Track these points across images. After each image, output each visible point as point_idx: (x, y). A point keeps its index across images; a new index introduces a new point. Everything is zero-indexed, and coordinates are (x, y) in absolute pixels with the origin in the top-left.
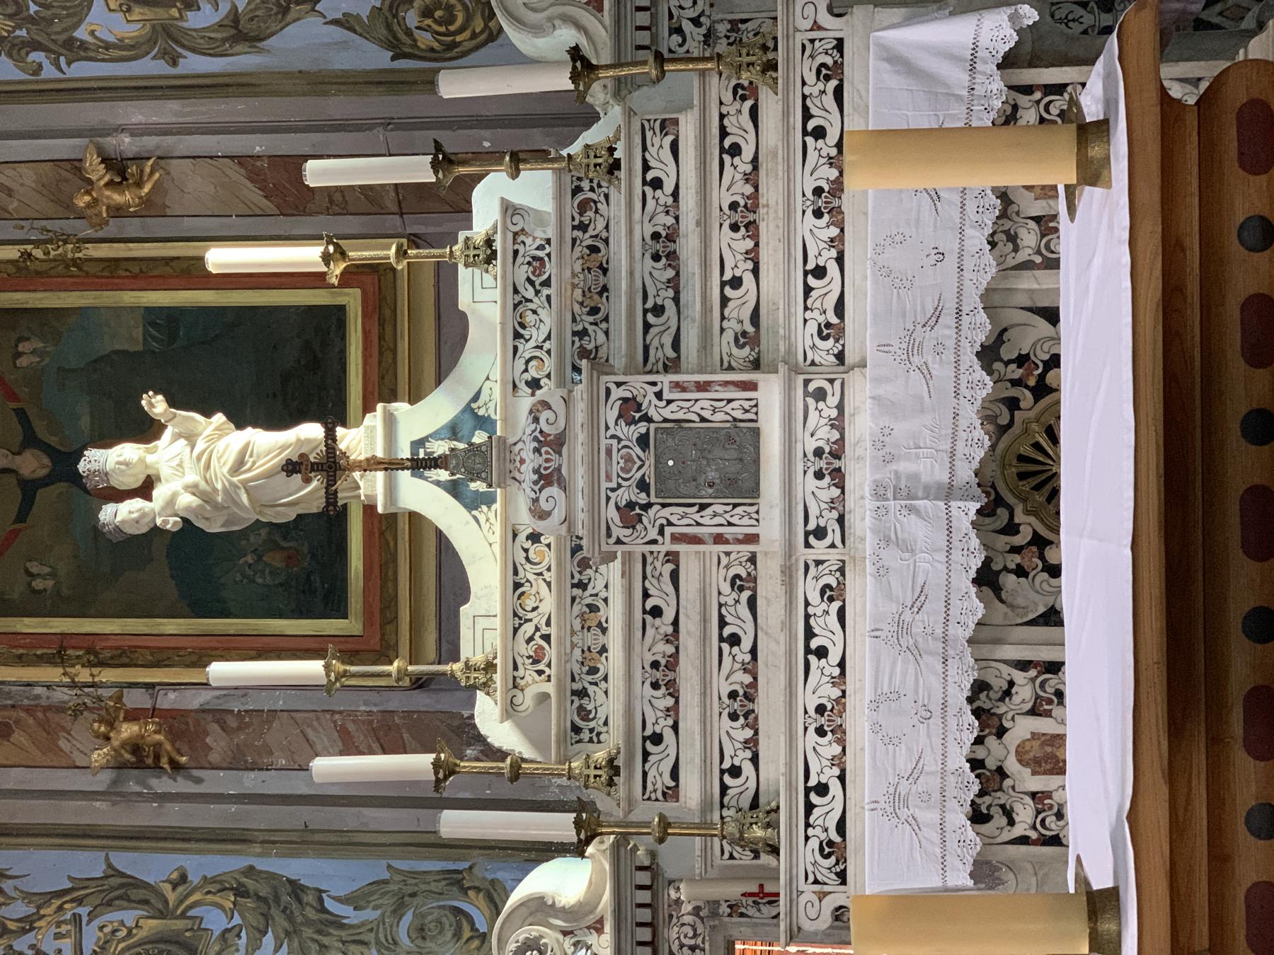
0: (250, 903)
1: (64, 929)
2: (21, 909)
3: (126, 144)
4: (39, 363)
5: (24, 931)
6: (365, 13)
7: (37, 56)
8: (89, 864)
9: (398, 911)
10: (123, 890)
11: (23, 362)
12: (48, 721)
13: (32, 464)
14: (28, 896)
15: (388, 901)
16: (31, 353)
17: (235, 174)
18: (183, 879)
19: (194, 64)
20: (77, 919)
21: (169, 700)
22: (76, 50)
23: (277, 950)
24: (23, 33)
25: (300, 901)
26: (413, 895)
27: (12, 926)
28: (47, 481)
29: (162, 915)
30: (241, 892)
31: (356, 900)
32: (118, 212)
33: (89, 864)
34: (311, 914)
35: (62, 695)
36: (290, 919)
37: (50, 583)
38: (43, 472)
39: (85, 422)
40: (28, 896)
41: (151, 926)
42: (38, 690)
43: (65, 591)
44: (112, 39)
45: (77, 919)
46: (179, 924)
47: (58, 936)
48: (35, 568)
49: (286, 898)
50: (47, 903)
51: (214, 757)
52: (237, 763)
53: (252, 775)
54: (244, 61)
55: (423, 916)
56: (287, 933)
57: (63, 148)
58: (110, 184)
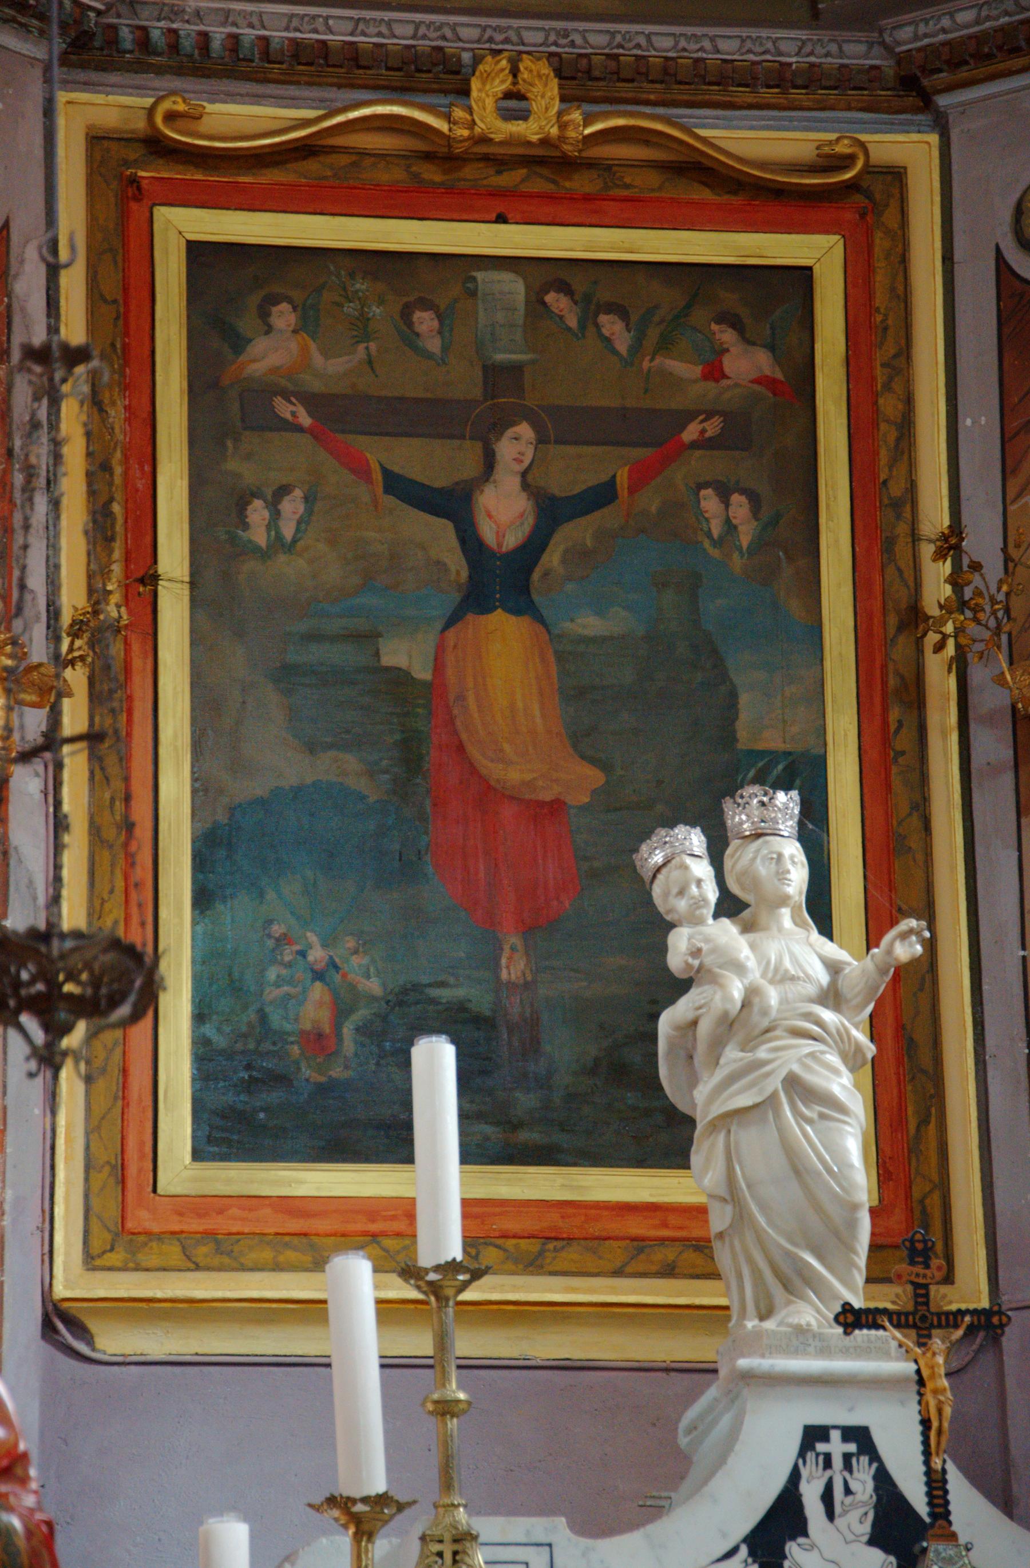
4: (709, 535)
11: (710, 502)
13: (503, 512)
16: (730, 517)
28: (471, 543)
37: (259, 536)
38: (488, 532)
39: (589, 624)
48: (292, 507)
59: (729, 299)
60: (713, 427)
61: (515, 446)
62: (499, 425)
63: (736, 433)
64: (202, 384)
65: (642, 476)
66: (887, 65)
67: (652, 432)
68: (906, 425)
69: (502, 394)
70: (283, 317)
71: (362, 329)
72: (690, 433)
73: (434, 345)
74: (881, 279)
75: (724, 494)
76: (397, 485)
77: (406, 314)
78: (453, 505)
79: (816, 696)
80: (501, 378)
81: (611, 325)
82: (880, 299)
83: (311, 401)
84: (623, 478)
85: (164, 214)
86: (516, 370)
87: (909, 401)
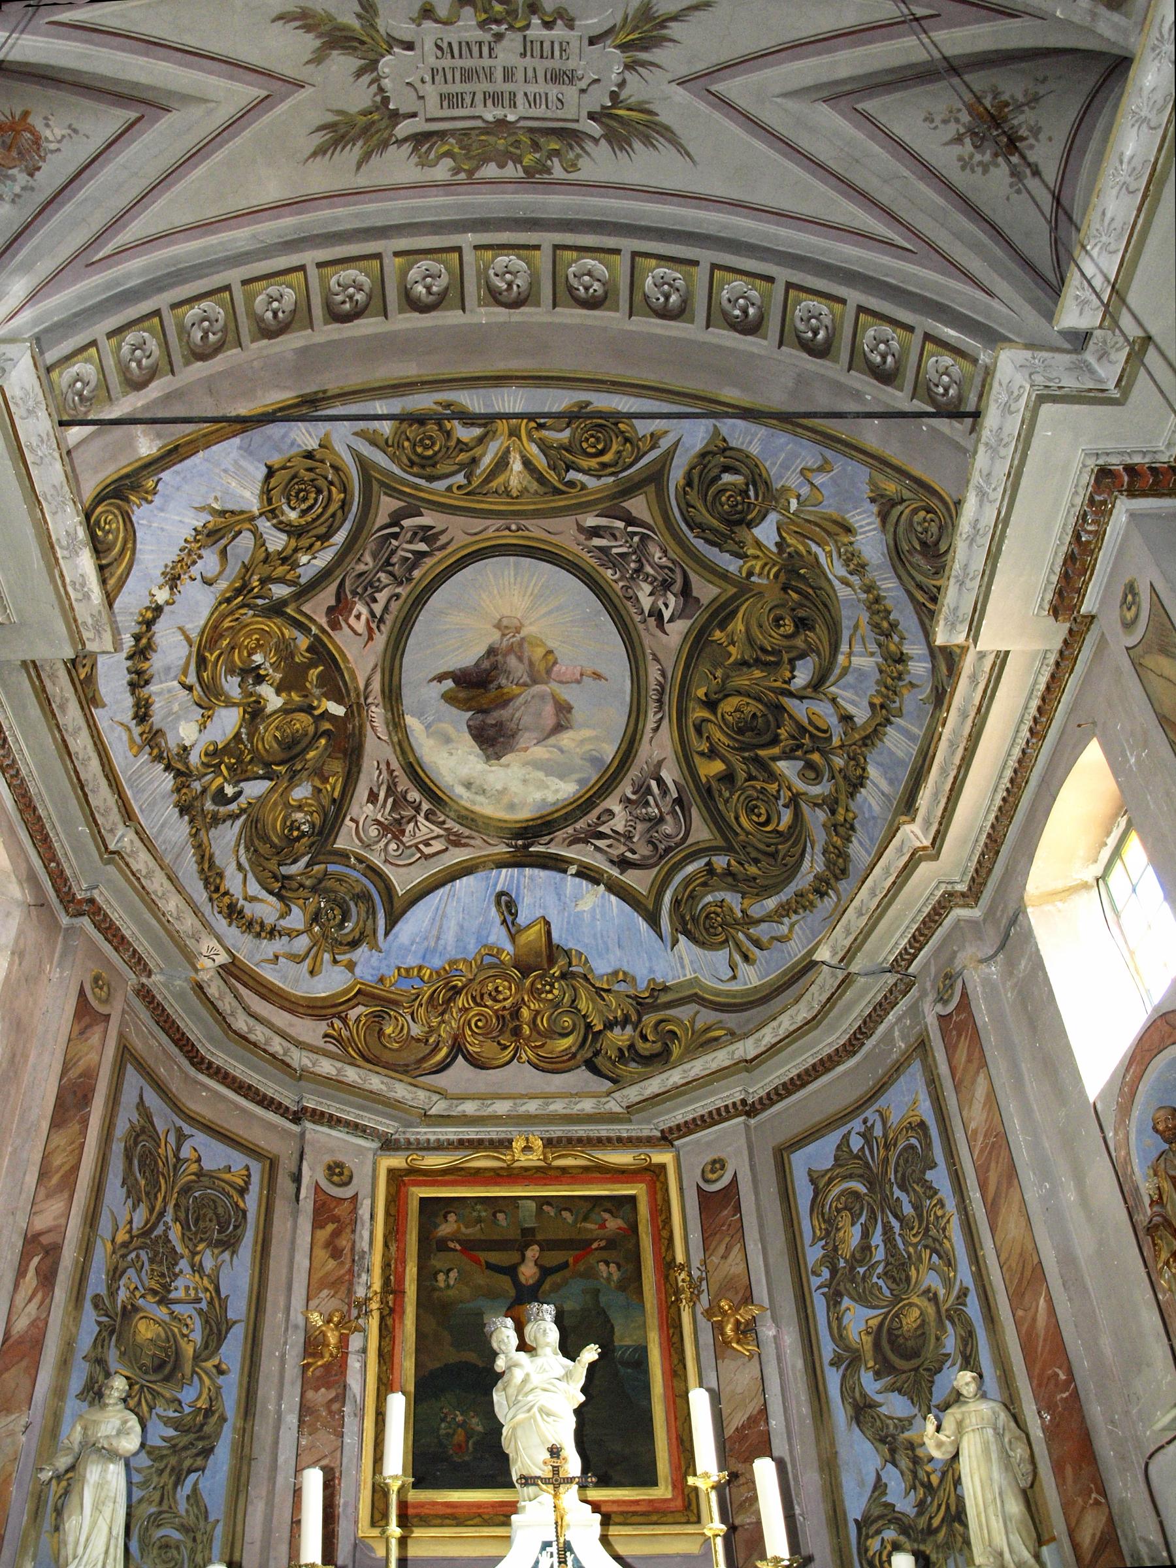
0: (200, 1419)
1: (192, 1292)
2: (208, 1264)
3: (768, 1331)
5: (193, 1266)
6: (889, 1499)
7: (826, 1274)
8: (238, 1308)
9: (185, 1529)
10: (216, 1330)
12: (343, 1283)
13: (528, 1272)
14: (217, 1268)
15: (191, 1520)
17: (753, 1408)
18: (221, 1372)
19: (833, 1379)
20: (198, 1300)
21: (354, 1363)
22: (834, 1299)
23: (164, 1439)
24: (842, 1264)
25: (197, 1455)
26: (194, 1540)
27: (197, 1258)
29: (197, 1358)
30: (209, 1412)
31: (195, 1494)
32: (718, 1328)
33: (238, 1308)
34: (187, 1463)
35: (360, 1292)
36: (185, 1448)
37: (442, 1285)
38: (523, 1279)
40: (217, 1268)
41: (189, 1350)
42: (364, 1277)
43: (436, 1294)
44: (845, 1321)
45: (198, 1300)
46: (188, 1368)
47: (187, 1288)
48: (453, 1275)
49: (200, 1445)
50: (212, 1282)
51: (310, 1394)
52: (305, 1410)
53: (295, 1421)
54: (840, 1413)
55: (178, 1548)
56: (174, 1446)
57: (761, 1292)
58: (738, 1322)
59: (608, 1205)
60: (603, 1243)
61: (533, 1252)
62: (527, 1246)
63: (611, 1244)
64: (423, 1239)
65: (577, 1260)
66: (659, 1134)
67: (582, 1245)
68: (671, 1239)
69: (527, 1237)
70: (452, 1217)
71: (479, 1220)
72: (595, 1246)
73: (504, 1223)
74: (659, 1197)
75: (607, 1264)
76: (490, 1266)
77: (494, 1215)
78: (511, 1271)
79: (644, 1326)
80: (526, 1232)
81: (566, 1214)
82: (660, 1202)
83: (459, 1241)
84: (571, 1260)
85: (414, 1189)
86: (532, 1230)
87: (671, 1232)
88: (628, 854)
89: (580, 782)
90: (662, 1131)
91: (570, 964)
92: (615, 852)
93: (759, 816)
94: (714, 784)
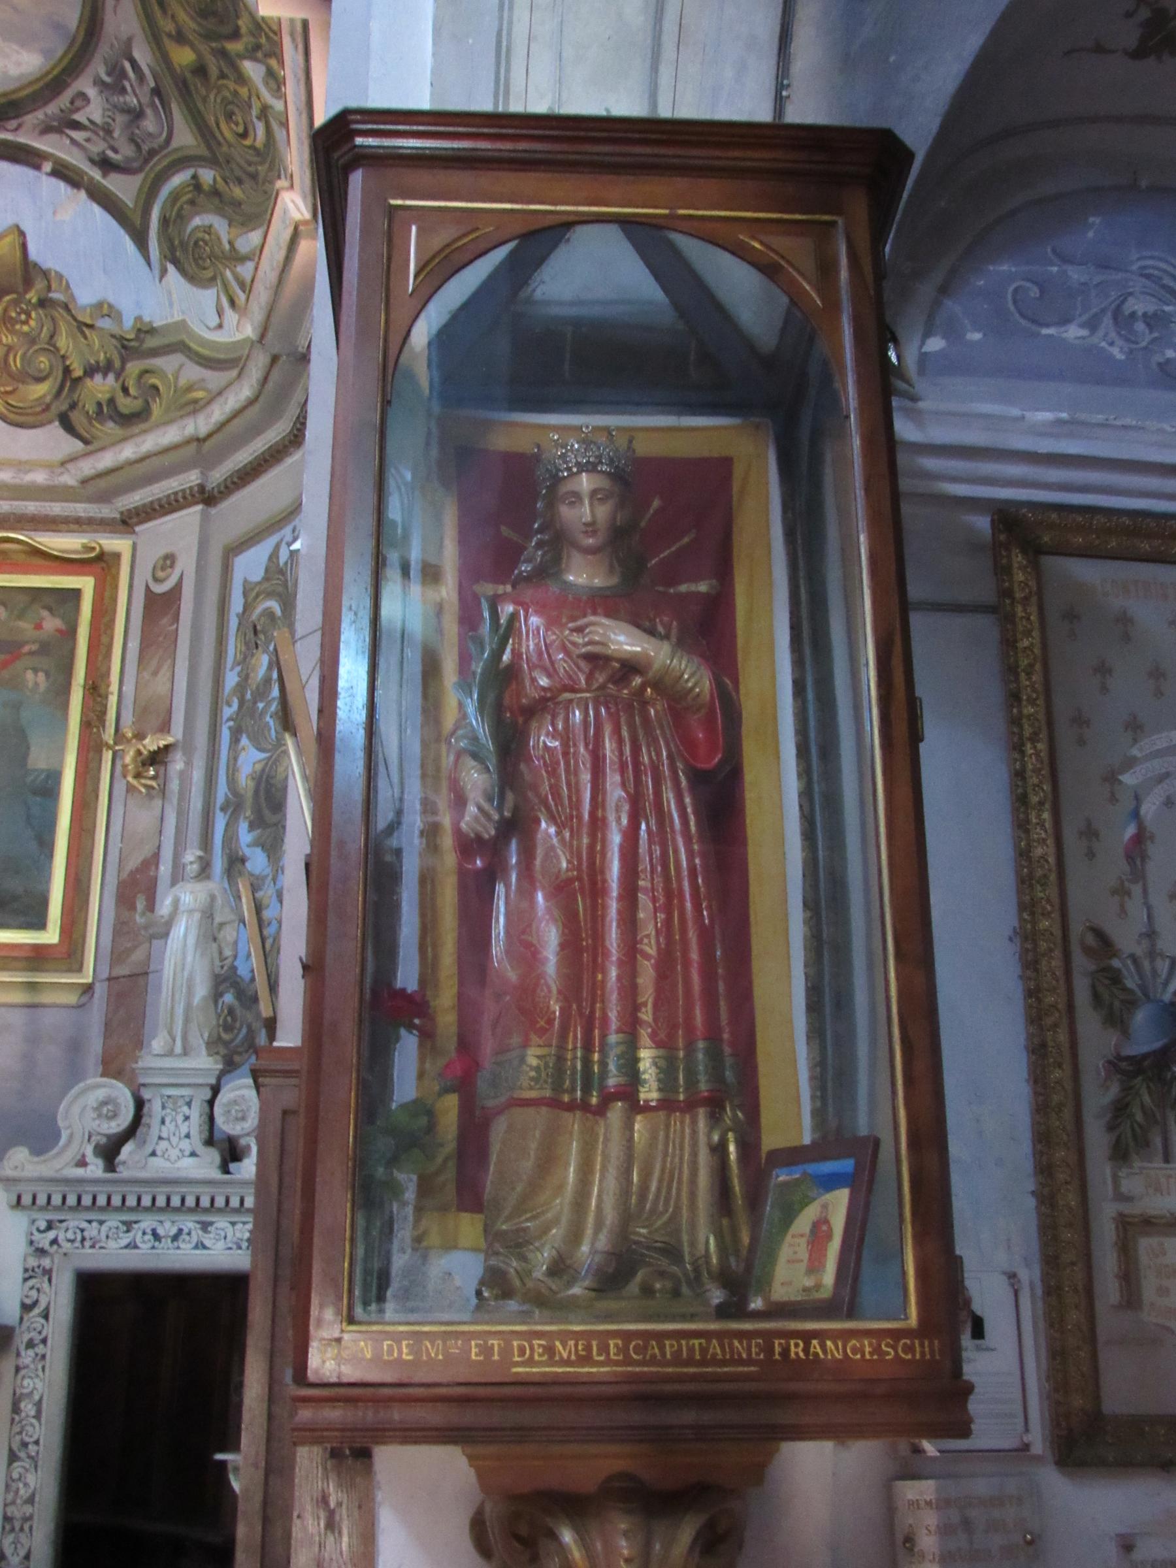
66: (118, 516)
88: (110, 153)
89: (46, 53)
90: (122, 513)
91: (49, 289)
92: (98, 147)
93: (237, 124)
94: (188, 75)
